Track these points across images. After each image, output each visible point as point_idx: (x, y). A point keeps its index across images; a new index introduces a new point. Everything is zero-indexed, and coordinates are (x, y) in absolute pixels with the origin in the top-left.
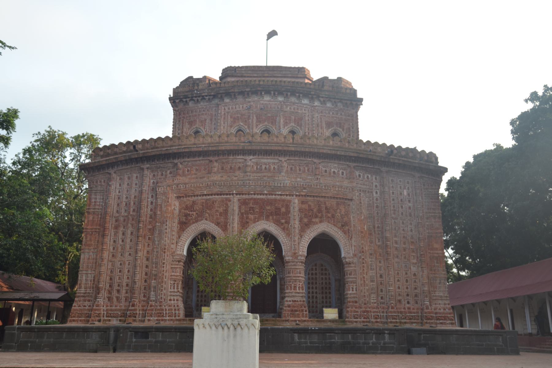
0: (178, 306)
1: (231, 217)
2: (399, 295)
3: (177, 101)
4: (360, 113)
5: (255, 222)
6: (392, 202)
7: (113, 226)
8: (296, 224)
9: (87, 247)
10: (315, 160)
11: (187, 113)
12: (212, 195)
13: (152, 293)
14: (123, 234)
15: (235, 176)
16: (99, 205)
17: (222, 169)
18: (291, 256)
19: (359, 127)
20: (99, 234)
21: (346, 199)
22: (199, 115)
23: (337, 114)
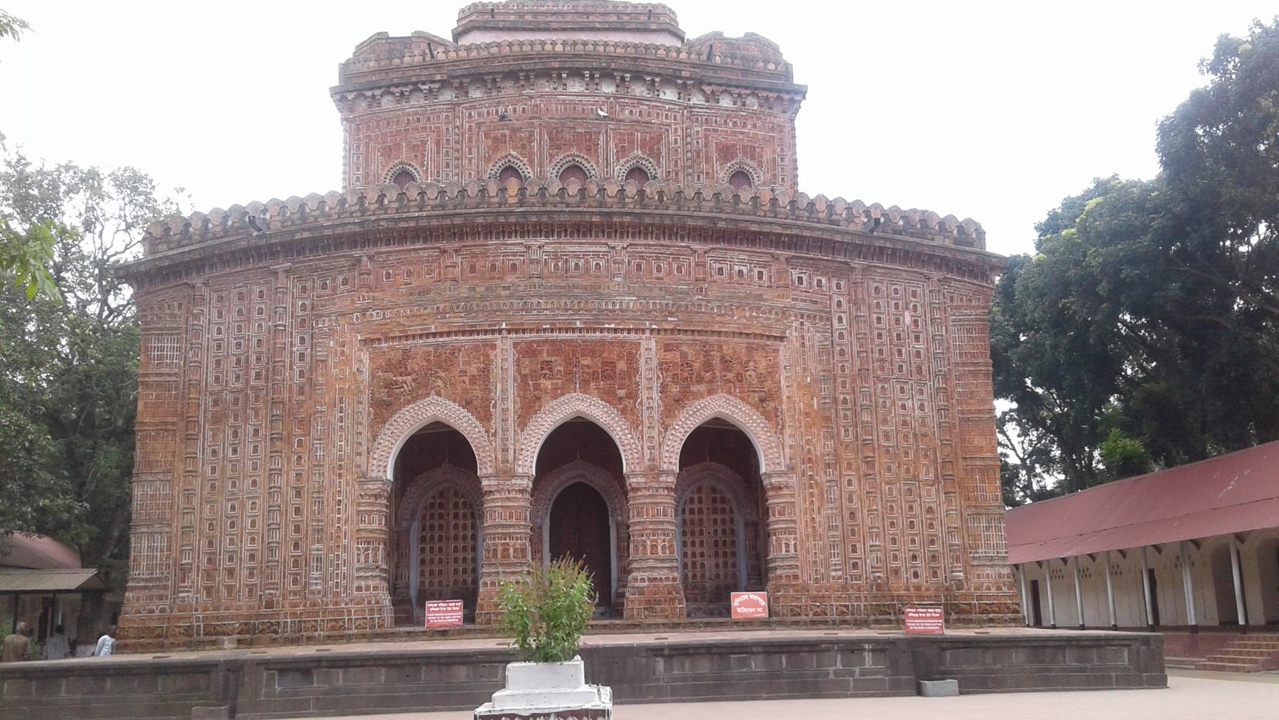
0: (377, 602)
1: (499, 387)
3: (351, 96)
4: (797, 123)
5: (555, 397)
6: (877, 341)
7: (209, 415)
8: (650, 397)
10: (695, 246)
11: (378, 126)
12: (449, 334)
14: (235, 434)
15: (505, 288)
17: (473, 269)
18: (644, 476)
21: (769, 337)
23: (745, 125)
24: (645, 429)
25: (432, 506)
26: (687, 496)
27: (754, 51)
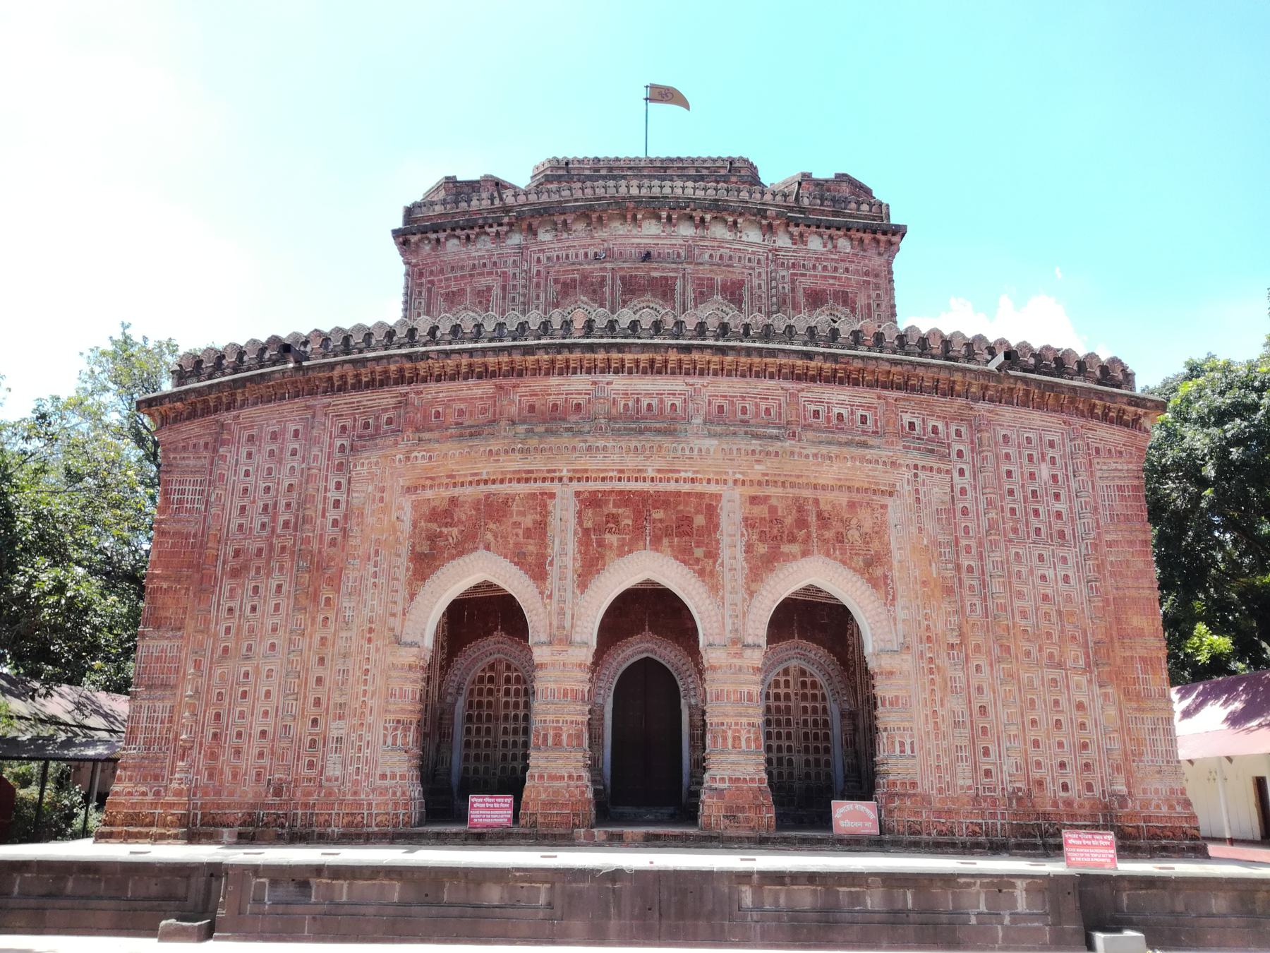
2: (1038, 764)
3: (414, 239)
4: (897, 265)
5: (621, 554)
13: (334, 757)
16: (190, 511)
19: (897, 302)
22: (471, 275)
23: (836, 269)
24: (727, 596)
25: (481, 679)
26: (772, 678)
27: (845, 190)
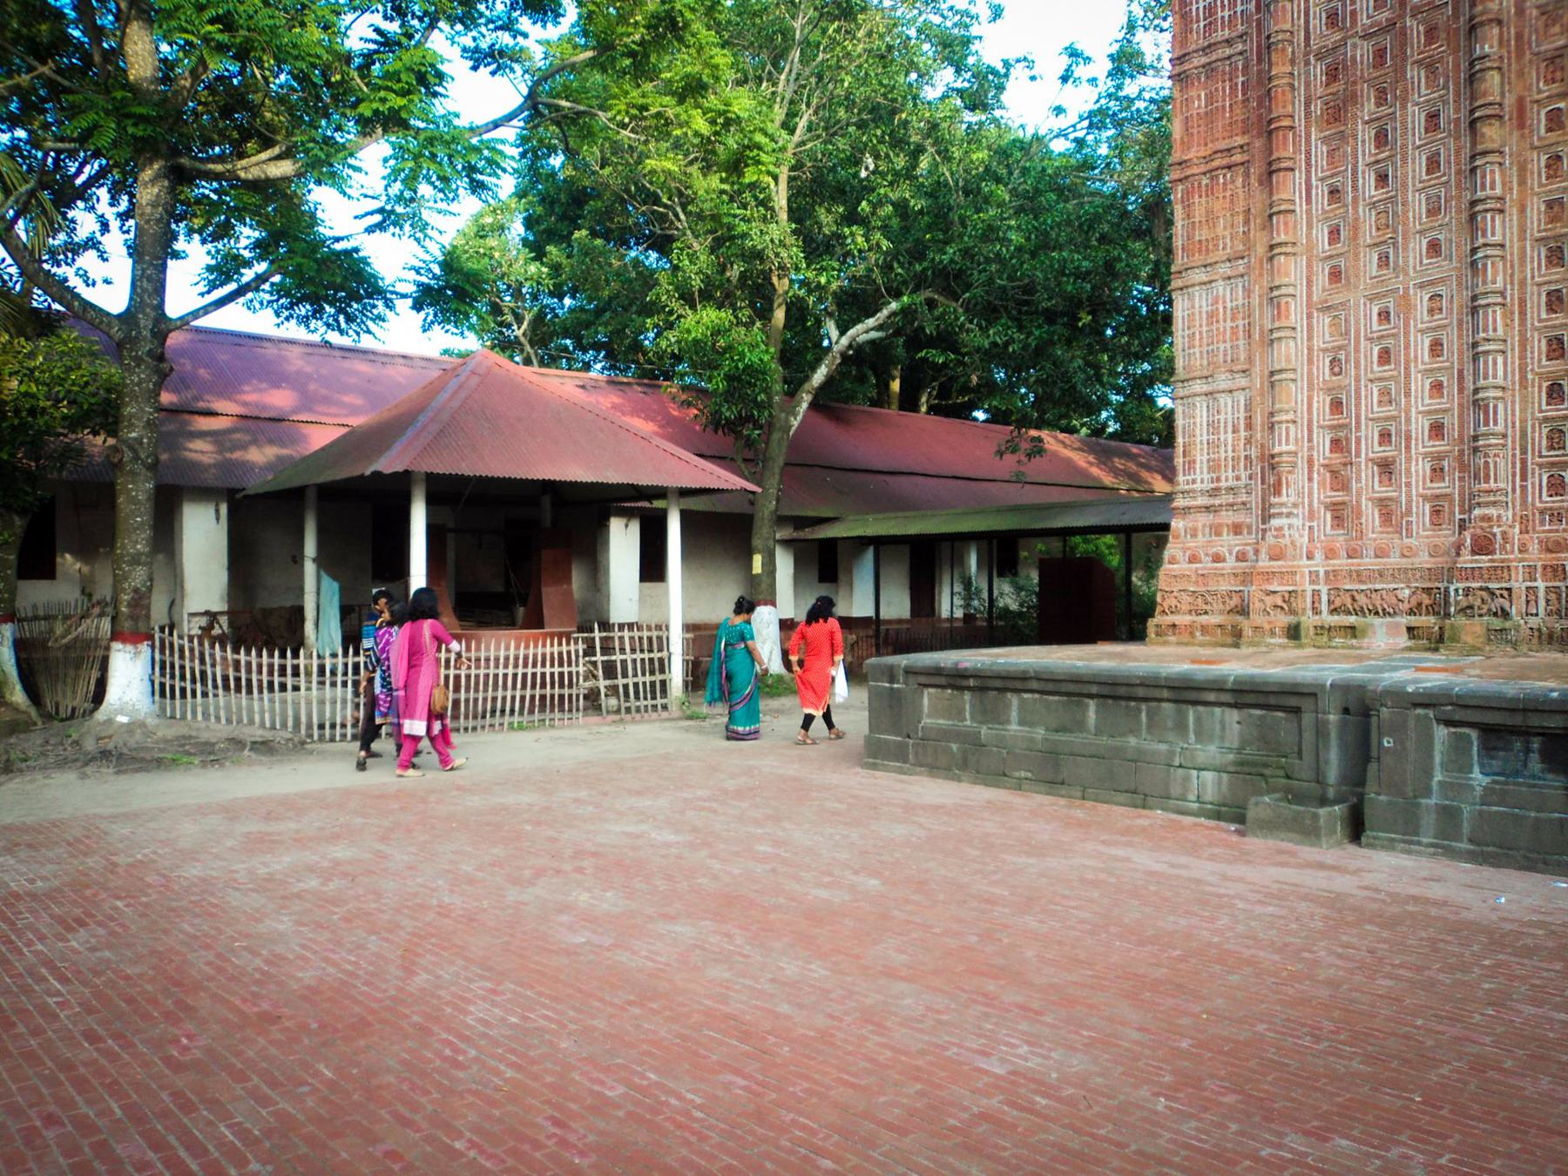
7: (1317, 107)
9: (1198, 259)
14: (1381, 139)
20: (1247, 175)
